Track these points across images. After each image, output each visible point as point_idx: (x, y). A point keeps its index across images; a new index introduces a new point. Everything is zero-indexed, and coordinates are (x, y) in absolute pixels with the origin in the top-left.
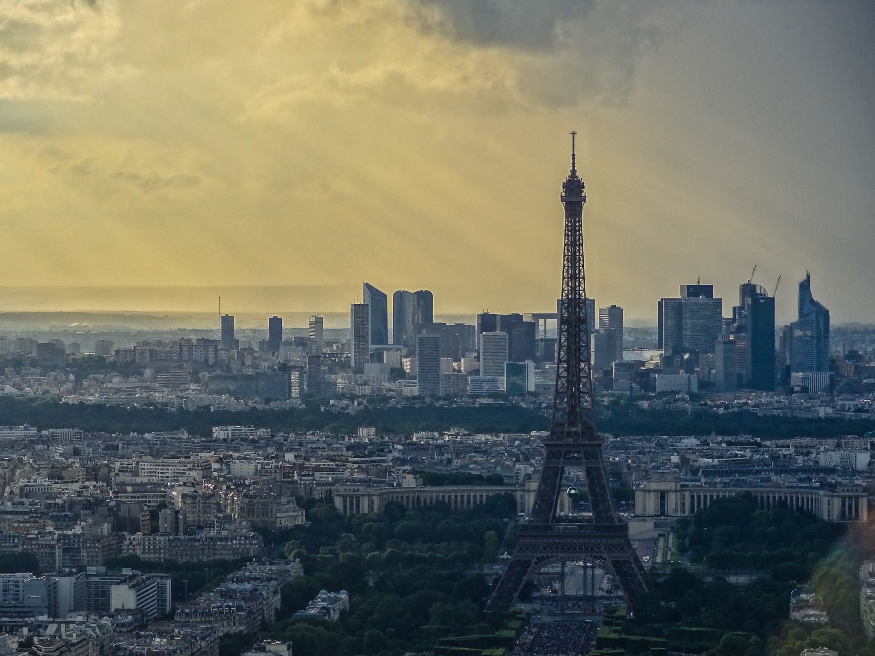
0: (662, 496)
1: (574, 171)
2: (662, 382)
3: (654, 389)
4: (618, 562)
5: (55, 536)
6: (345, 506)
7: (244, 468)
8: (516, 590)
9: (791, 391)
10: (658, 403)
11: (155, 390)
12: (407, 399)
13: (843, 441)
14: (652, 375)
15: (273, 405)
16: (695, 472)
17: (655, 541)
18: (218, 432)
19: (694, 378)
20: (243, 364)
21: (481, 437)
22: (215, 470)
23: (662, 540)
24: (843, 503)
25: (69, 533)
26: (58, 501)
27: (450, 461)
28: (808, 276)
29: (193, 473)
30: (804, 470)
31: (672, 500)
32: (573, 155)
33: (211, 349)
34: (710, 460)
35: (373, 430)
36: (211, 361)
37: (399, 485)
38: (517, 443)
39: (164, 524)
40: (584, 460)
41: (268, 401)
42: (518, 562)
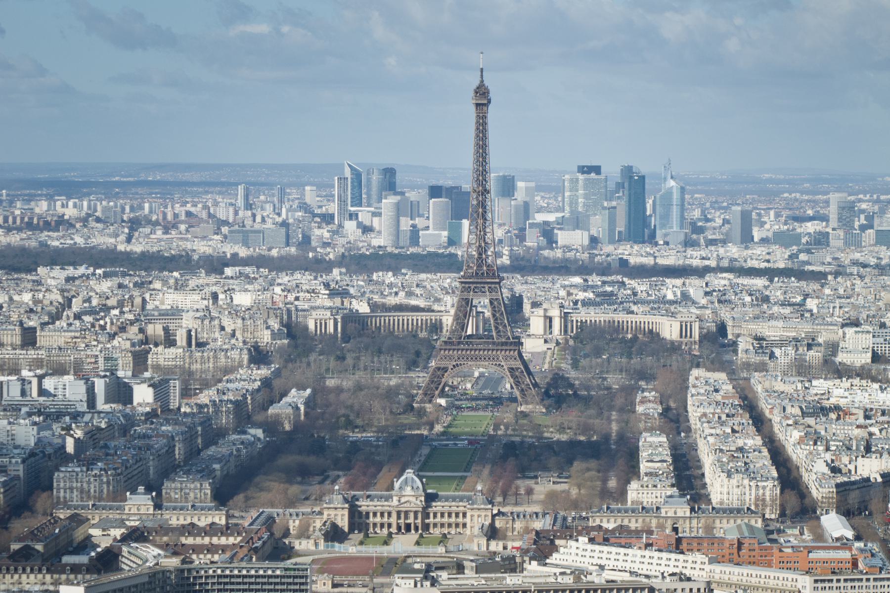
0: (551, 319)
1: (482, 81)
2: (563, 237)
3: (556, 242)
4: (512, 369)
5: (99, 348)
6: (316, 327)
7: (243, 299)
8: (437, 388)
9: (656, 244)
10: (559, 254)
11: (187, 240)
12: (374, 247)
13: (687, 281)
14: (556, 231)
15: (274, 253)
16: (576, 303)
17: (545, 353)
18: (229, 271)
19: (586, 234)
20: (254, 221)
21: (423, 276)
22: (222, 300)
23: (549, 351)
24: (681, 326)
25: (109, 346)
26: (102, 322)
27: (396, 294)
28: (670, 160)
29: (206, 302)
30: (654, 302)
31: (556, 323)
32: (482, 70)
33: (231, 210)
34: (586, 294)
35: (344, 270)
36: (231, 220)
37: (357, 311)
38: (448, 281)
39: (181, 337)
40: (488, 293)
41: (270, 249)
42: (439, 369)
